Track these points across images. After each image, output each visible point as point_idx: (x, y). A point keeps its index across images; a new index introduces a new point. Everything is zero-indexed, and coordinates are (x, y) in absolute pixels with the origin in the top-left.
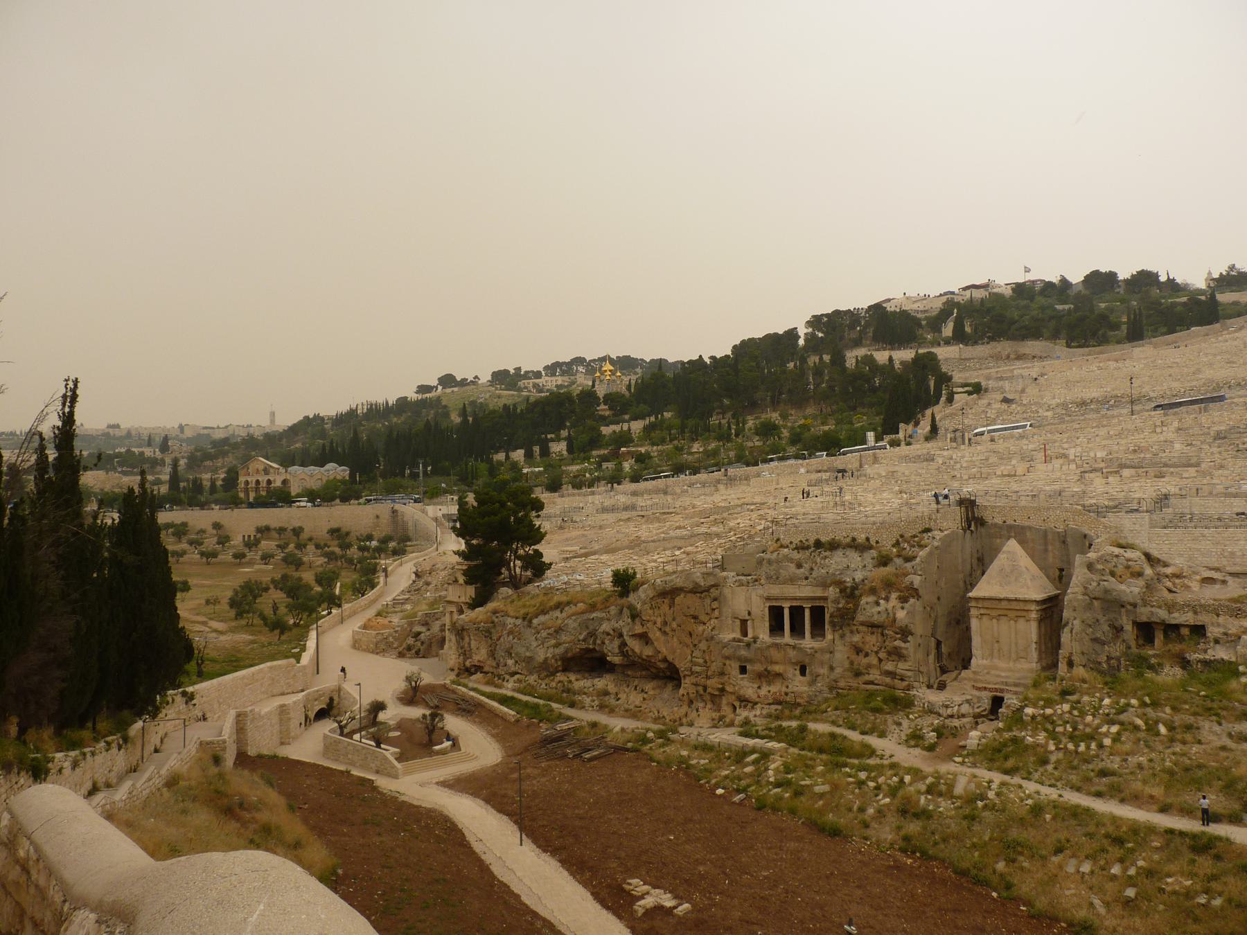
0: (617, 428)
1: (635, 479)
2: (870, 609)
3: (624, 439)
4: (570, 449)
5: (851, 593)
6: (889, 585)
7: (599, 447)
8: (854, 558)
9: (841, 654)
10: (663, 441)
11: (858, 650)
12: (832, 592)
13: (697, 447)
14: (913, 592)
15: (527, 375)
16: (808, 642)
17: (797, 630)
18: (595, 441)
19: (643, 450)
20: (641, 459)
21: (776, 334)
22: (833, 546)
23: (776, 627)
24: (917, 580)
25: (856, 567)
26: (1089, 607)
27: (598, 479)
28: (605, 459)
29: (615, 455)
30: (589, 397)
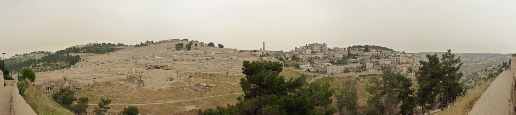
0: (39, 64)
1: (40, 72)
2: (54, 88)
3: (39, 66)
4: (33, 67)
5: (53, 86)
6: (56, 85)
7: (37, 67)
8: (53, 83)
9: (52, 91)
10: (44, 66)
11: (53, 91)
12: (51, 86)
13: (49, 67)
14: (58, 86)
15: (28, 54)
16: (49, 91)
17: (49, 89)
18: (36, 66)
19: (42, 67)
20: (41, 69)
21: (59, 51)
22: (52, 82)
23: (47, 89)
24: (58, 85)
25: (53, 84)
26: (72, 87)
27: (35, 72)
28: (37, 69)
29: (38, 68)
30: (35, 60)
